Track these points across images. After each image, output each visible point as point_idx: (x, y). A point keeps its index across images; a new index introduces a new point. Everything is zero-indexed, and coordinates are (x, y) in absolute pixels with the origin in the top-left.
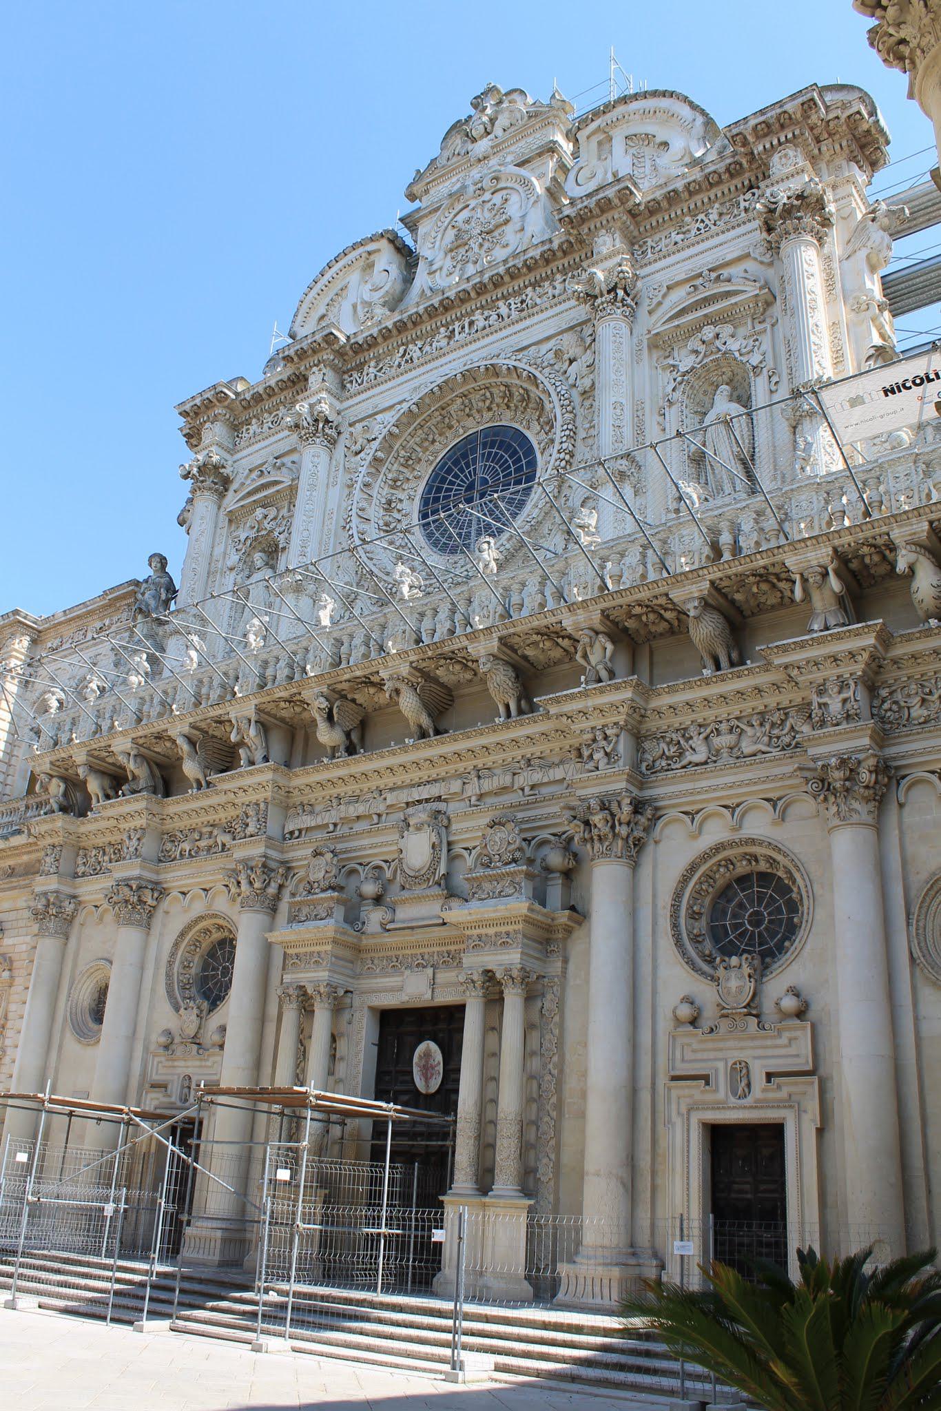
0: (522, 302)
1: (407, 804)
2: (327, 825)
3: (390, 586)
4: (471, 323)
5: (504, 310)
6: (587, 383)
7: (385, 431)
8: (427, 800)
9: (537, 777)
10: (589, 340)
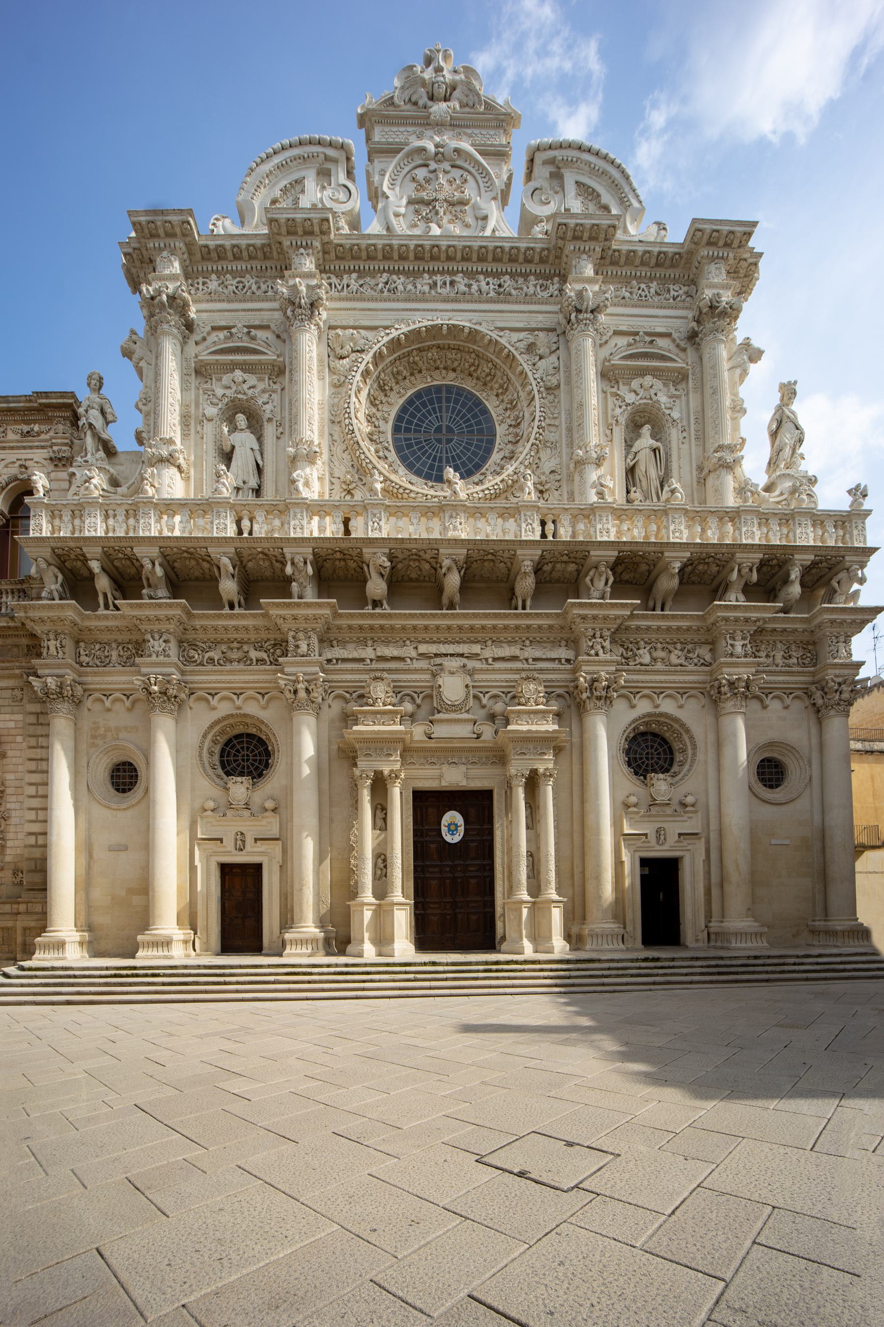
0: (500, 286)
1: (435, 654)
2: (362, 660)
3: (397, 487)
4: (452, 283)
5: (484, 287)
6: (554, 381)
7: (376, 348)
8: (452, 655)
9: (538, 654)
10: (554, 347)
